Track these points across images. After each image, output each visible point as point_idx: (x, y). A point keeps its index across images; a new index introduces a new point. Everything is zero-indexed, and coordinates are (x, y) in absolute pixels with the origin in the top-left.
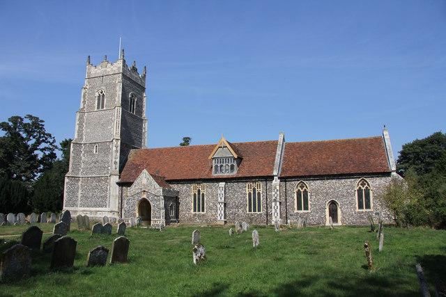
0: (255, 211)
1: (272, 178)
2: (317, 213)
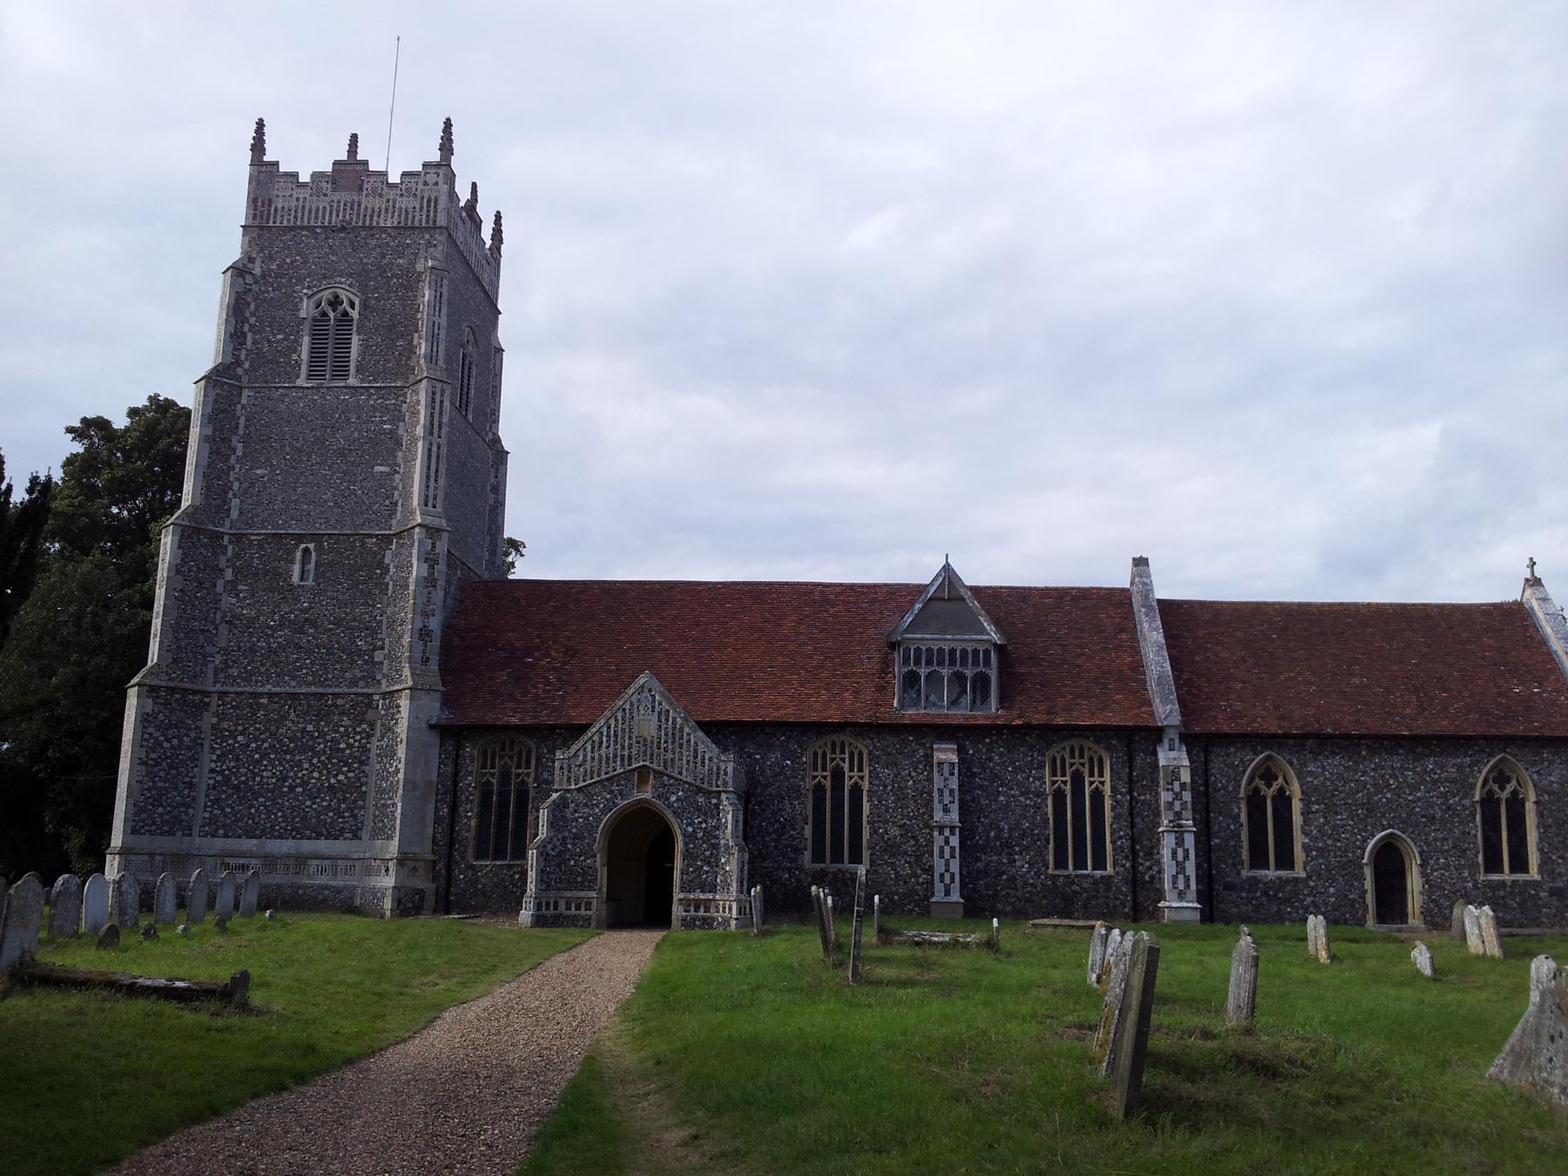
0: (1080, 863)
1: (1155, 734)
2: (1332, 880)
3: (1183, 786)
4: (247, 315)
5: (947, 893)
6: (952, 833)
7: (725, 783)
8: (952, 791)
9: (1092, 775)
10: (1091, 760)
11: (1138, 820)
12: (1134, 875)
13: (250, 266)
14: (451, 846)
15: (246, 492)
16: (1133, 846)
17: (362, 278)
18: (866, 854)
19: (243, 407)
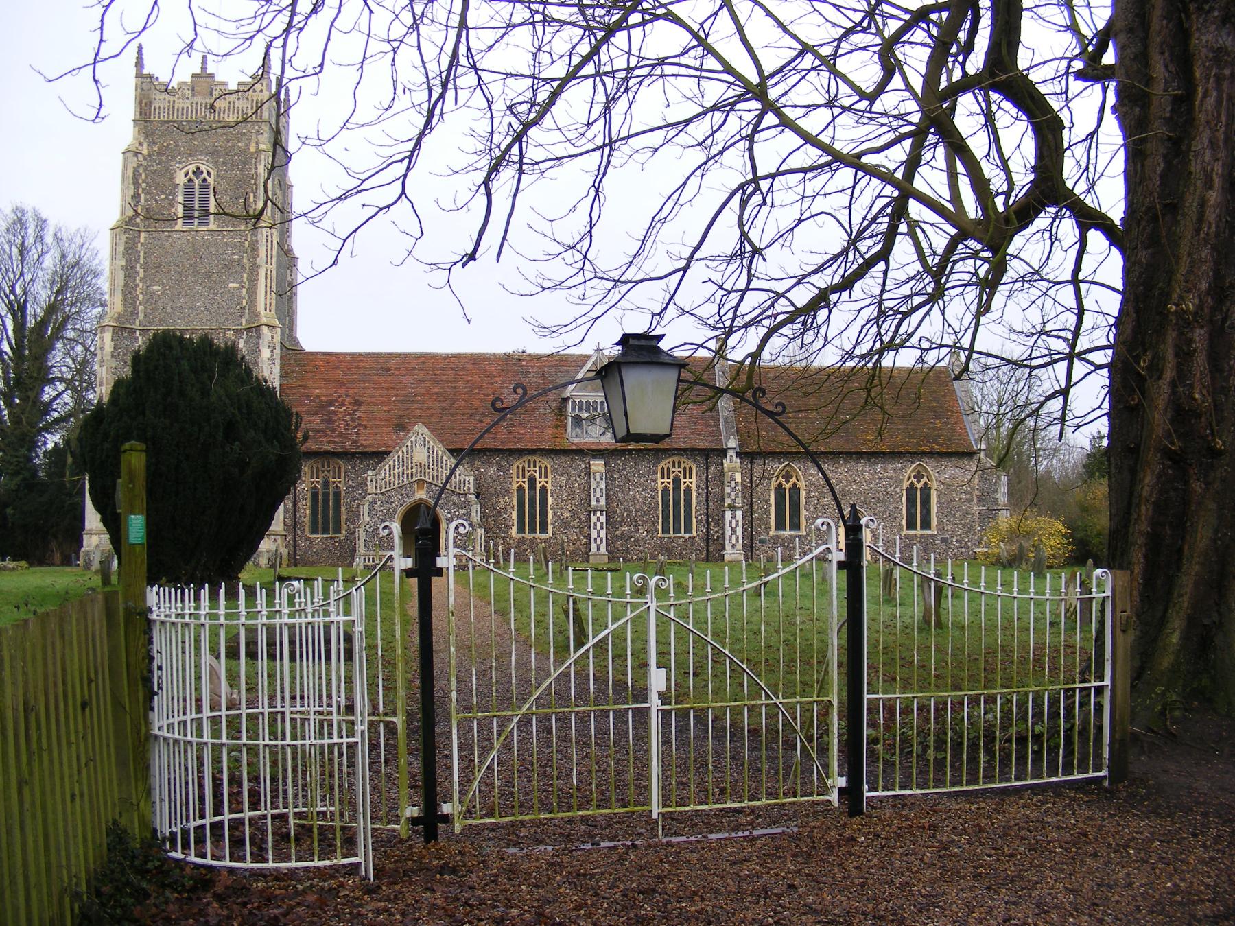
0: (677, 530)
1: (723, 452)
3: (737, 483)
4: (140, 181)
5: (599, 549)
6: (601, 514)
7: (469, 488)
8: (601, 490)
9: (685, 478)
10: (685, 468)
11: (711, 504)
12: (708, 535)
13: (140, 148)
14: (295, 527)
15: (147, 301)
16: (707, 520)
17: (214, 155)
18: (550, 528)
19: (142, 244)
